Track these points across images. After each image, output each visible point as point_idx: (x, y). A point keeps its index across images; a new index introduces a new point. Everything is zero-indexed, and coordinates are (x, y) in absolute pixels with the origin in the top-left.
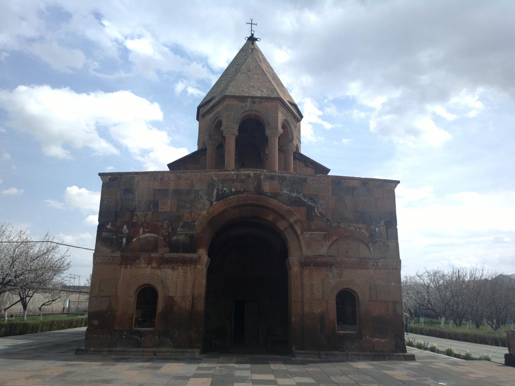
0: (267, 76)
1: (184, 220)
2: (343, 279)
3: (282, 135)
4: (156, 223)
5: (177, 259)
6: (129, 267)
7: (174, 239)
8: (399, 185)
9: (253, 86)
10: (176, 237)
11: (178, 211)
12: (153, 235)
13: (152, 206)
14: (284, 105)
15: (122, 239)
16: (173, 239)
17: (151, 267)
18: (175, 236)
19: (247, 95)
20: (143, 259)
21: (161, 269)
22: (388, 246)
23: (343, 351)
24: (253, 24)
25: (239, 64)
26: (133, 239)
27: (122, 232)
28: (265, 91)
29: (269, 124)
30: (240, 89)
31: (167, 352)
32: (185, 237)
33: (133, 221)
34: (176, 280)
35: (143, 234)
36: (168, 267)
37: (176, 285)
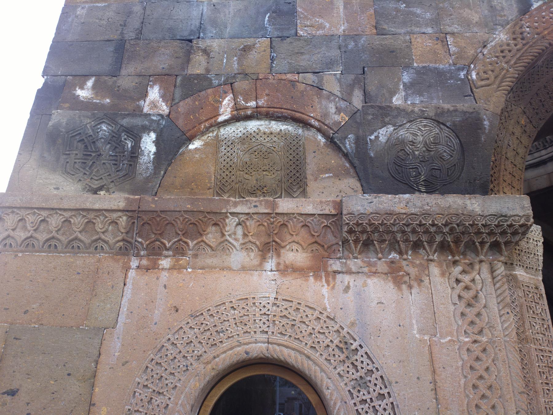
1: (415, 65)
4: (289, 76)
5: (420, 225)
6: (165, 263)
7: (383, 139)
10: (391, 128)
11: (381, 32)
12: (276, 126)
13: (267, 18)
15: (137, 140)
16: (377, 137)
17: (278, 264)
18: (384, 124)
20: (239, 224)
21: (334, 278)
26: (190, 139)
27: (138, 112)
32: (437, 130)
33: (190, 72)
34: (426, 337)
35: (235, 119)
36: (366, 270)
37: (434, 372)
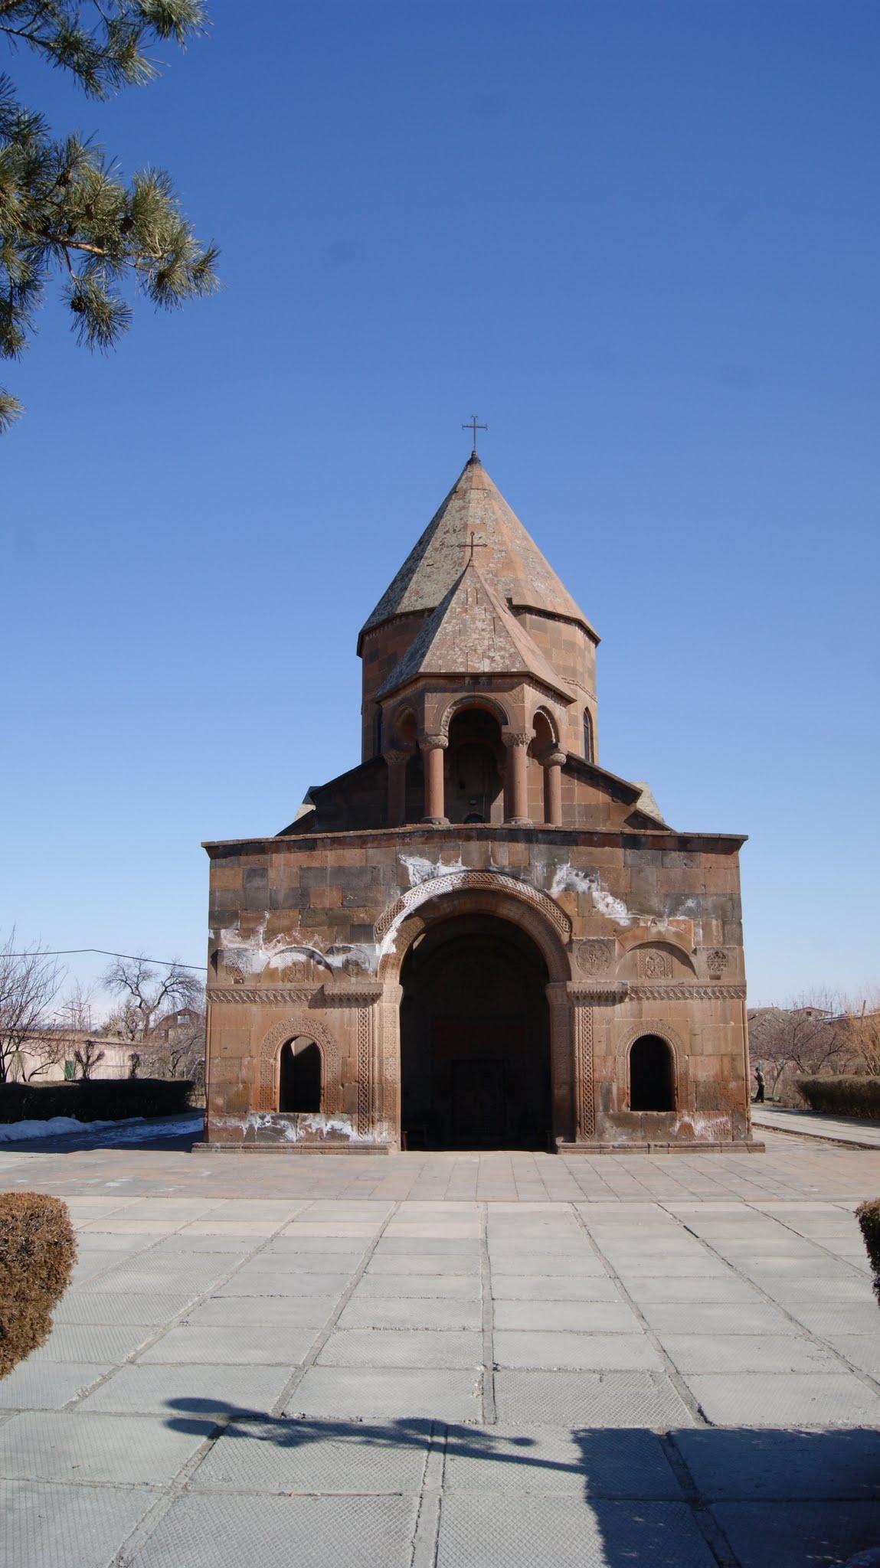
0: (501, 621)
2: (643, 1019)
3: (533, 741)
8: (745, 843)
9: (473, 648)
14: (536, 681)
19: (462, 670)
22: (724, 957)
23: (644, 1138)
24: (478, 427)
25: (448, 532)
28: (499, 657)
29: (507, 724)
30: (449, 658)
31: (341, 1148)
